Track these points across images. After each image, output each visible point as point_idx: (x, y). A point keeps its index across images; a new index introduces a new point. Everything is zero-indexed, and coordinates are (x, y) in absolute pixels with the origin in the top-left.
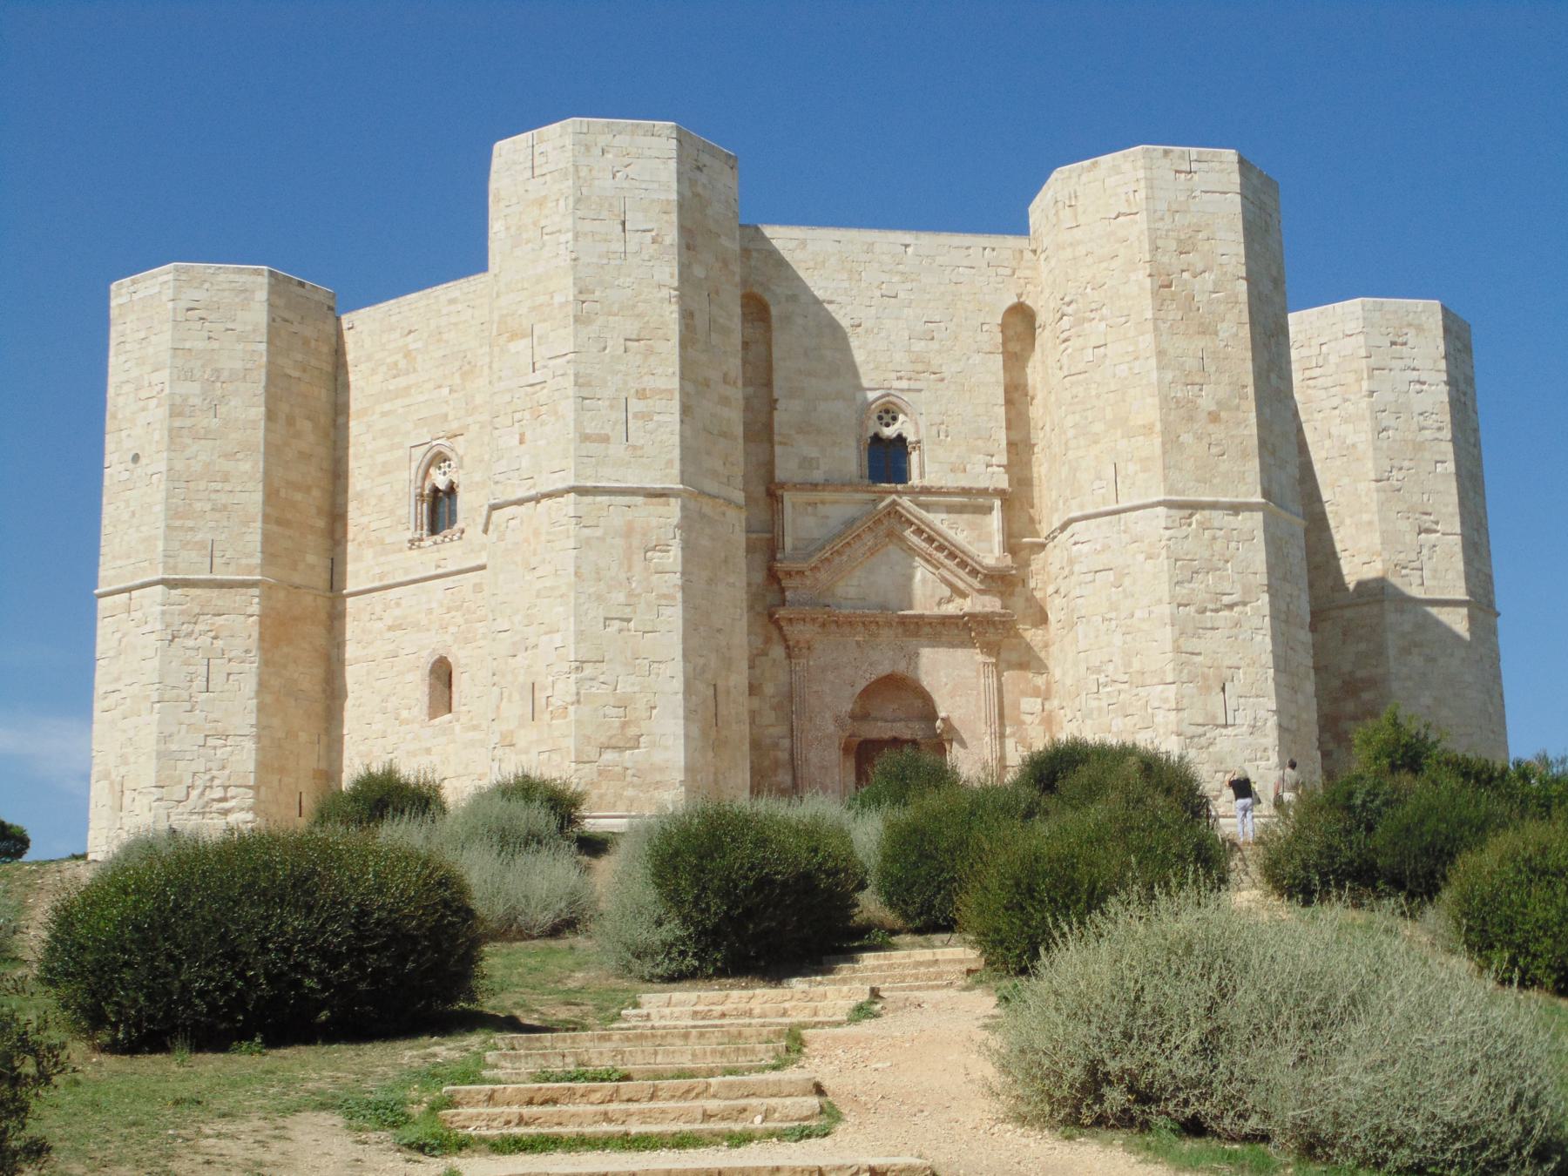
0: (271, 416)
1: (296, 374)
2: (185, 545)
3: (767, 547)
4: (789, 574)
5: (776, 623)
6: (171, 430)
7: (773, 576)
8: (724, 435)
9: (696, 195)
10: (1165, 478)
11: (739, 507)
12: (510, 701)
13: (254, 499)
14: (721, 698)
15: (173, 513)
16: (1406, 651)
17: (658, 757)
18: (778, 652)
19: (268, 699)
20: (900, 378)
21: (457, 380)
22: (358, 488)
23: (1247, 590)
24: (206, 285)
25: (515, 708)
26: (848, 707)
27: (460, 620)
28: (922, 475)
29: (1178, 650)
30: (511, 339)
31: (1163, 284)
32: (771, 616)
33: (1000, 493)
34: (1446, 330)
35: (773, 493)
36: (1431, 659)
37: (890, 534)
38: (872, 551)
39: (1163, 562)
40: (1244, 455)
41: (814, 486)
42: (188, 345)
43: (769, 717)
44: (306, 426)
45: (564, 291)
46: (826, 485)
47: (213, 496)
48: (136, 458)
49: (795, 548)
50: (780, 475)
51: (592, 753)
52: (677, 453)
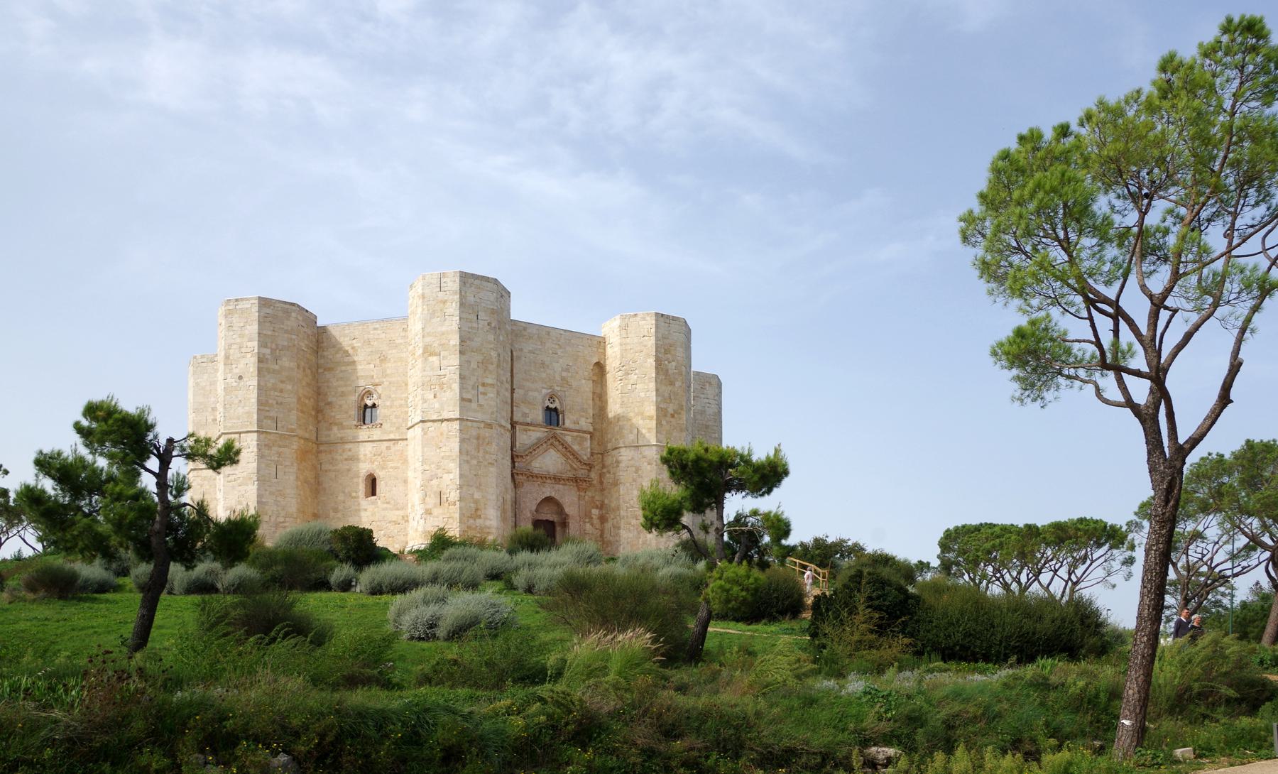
0: (298, 367)
2: (266, 417)
13: (292, 400)
15: (261, 403)
17: (488, 523)
25: (432, 501)
40: (681, 430)
48: (240, 377)
50: (515, 419)
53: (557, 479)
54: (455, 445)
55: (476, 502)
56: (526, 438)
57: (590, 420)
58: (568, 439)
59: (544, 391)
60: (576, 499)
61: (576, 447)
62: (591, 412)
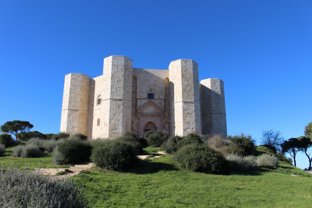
1: (84, 86)
3: (135, 106)
4: (138, 109)
5: (136, 115)
6: (70, 92)
7: (136, 110)
8: (129, 93)
9: (127, 64)
10: (182, 98)
11: (131, 101)
14: (127, 124)
15: (69, 101)
16: (215, 119)
17: (119, 131)
18: (136, 119)
19: (80, 123)
20: (152, 86)
23: (192, 112)
26: (144, 125)
28: (154, 98)
29: (183, 119)
30: (104, 81)
31: (183, 76)
32: (135, 114)
33: (163, 100)
34: (220, 82)
35: (136, 100)
36: (218, 121)
37: (150, 105)
38: (148, 107)
39: (182, 109)
41: (141, 99)
43: (135, 126)
44: (86, 92)
45: (110, 76)
46: (143, 99)
48: (66, 95)
49: (139, 106)
50: (137, 98)
51: (110, 130)
52: (123, 95)
53: (152, 115)
54: (109, 107)
55: (115, 125)
56: (140, 103)
57: (164, 96)
58: (156, 102)
59: (147, 88)
60: (160, 122)
61: (159, 105)
62: (164, 93)
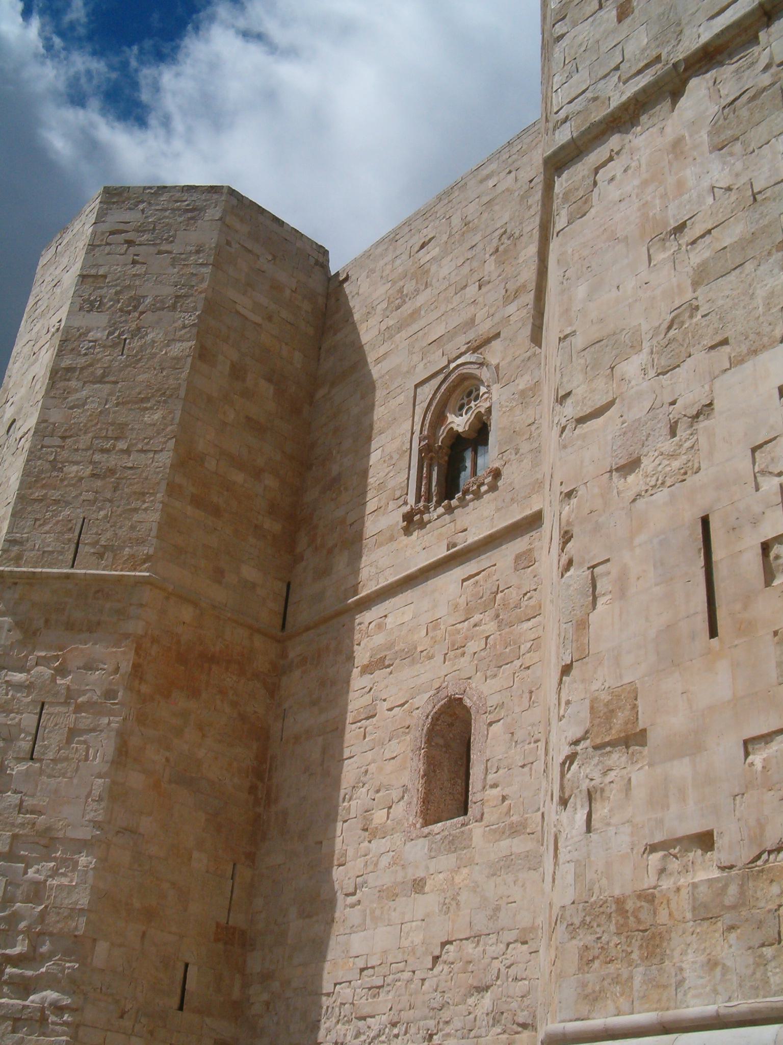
0: (203, 354)
12: (622, 592)
19: (136, 780)
21: (491, 266)
22: (335, 470)
24: (141, 206)
27: (490, 627)
42: (101, 272)
47: (97, 457)
